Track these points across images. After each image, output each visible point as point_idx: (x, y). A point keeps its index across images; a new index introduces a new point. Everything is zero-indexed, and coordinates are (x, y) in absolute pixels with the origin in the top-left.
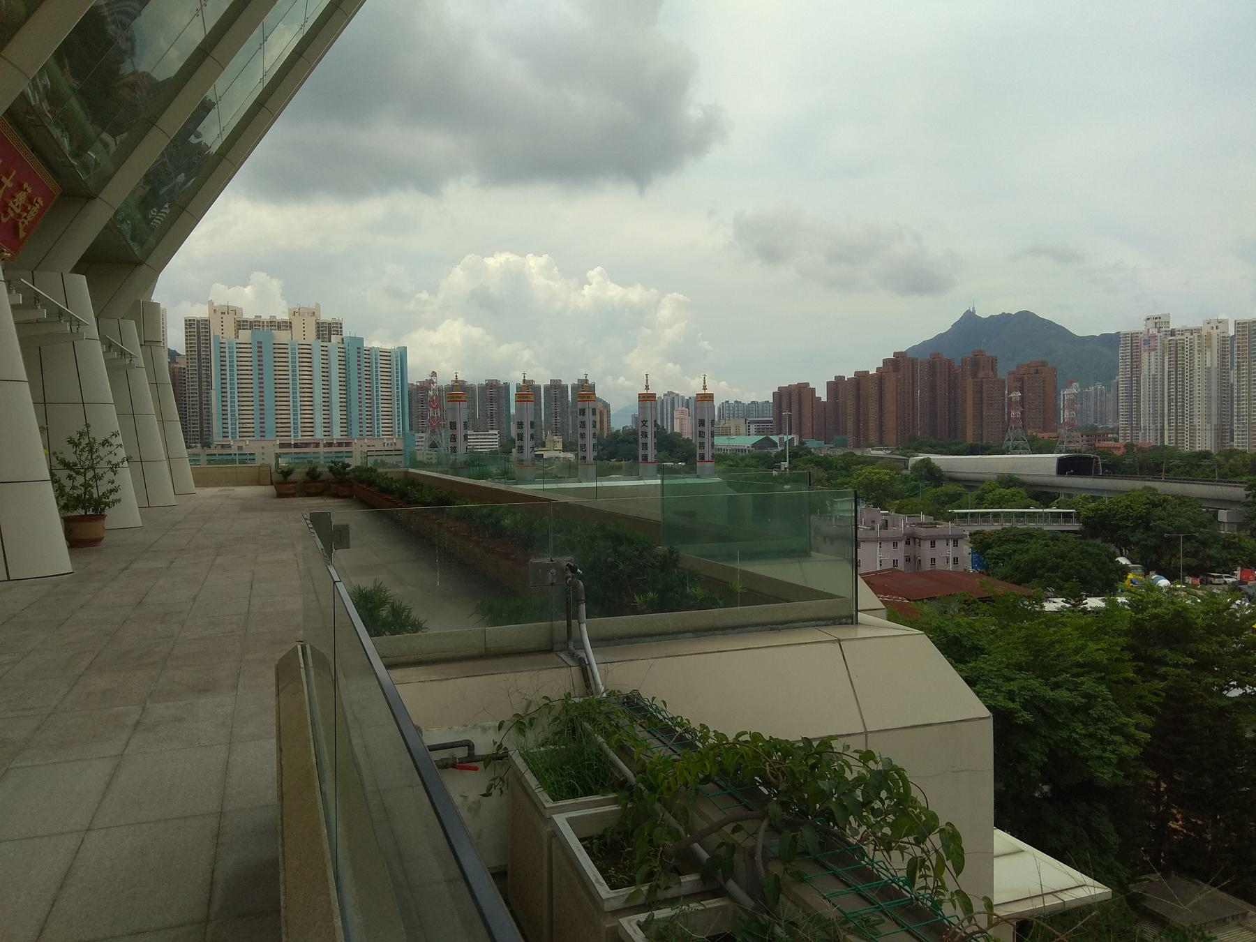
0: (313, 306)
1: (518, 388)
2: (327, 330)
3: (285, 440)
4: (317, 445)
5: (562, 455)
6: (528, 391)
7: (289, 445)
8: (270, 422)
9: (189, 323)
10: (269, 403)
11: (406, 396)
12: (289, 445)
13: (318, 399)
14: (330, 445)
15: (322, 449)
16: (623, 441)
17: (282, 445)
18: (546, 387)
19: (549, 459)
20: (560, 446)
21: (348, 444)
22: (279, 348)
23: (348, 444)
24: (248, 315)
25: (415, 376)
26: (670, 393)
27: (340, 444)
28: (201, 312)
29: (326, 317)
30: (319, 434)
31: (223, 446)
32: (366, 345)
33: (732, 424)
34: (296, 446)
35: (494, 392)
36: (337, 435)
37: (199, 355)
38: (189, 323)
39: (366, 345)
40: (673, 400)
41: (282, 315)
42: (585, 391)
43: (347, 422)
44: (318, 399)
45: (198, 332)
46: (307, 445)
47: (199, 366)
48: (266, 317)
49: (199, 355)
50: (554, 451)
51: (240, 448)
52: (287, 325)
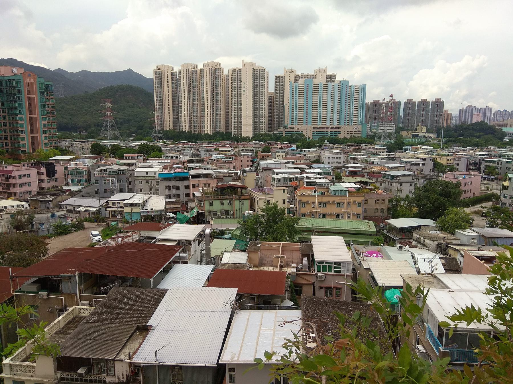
0: (324, 68)
1: (405, 104)
2: (331, 78)
3: (315, 126)
4: (327, 128)
5: (427, 135)
6: (409, 104)
7: (317, 128)
8: (310, 119)
9: (277, 77)
10: (310, 110)
11: (364, 108)
12: (317, 128)
13: (329, 109)
14: (332, 128)
15: (329, 130)
16: (466, 128)
17: (314, 128)
18: (419, 103)
19: (421, 136)
20: (425, 130)
21: (339, 128)
22: (316, 86)
23: (339, 128)
24: (299, 73)
25: (369, 99)
26: (470, 106)
27: (336, 128)
28: (281, 73)
29: (329, 72)
30: (329, 124)
31: (291, 128)
32: (350, 84)
33: (509, 121)
34: (319, 128)
35: (394, 105)
36: (335, 124)
37: (280, 91)
38: (277, 77)
39: (350, 84)
40: (472, 109)
41: (312, 73)
42: (439, 104)
43: (339, 120)
44: (329, 109)
45: (280, 81)
46: (323, 128)
47: (279, 95)
48: (305, 74)
49: (280, 91)
50: (422, 131)
51: (298, 129)
52: (315, 77)
